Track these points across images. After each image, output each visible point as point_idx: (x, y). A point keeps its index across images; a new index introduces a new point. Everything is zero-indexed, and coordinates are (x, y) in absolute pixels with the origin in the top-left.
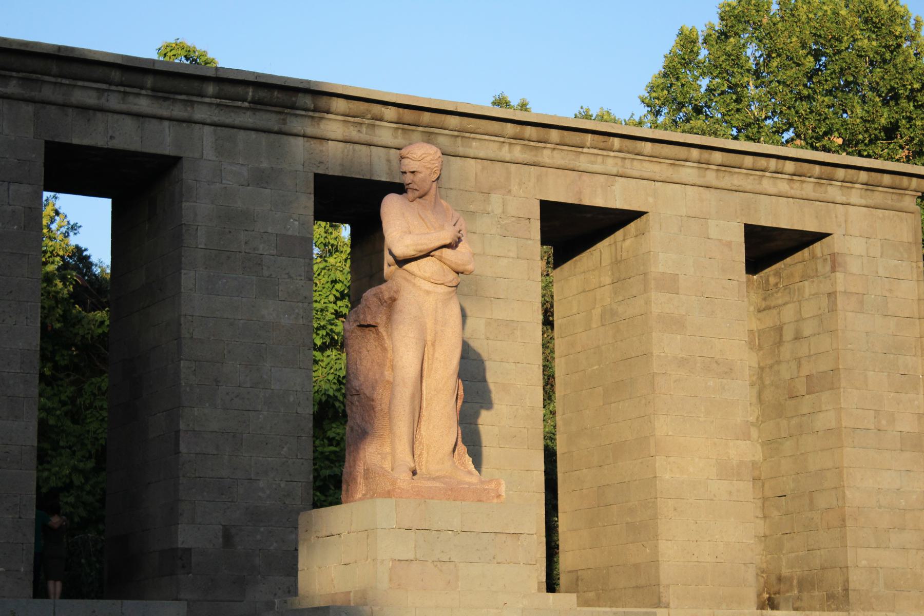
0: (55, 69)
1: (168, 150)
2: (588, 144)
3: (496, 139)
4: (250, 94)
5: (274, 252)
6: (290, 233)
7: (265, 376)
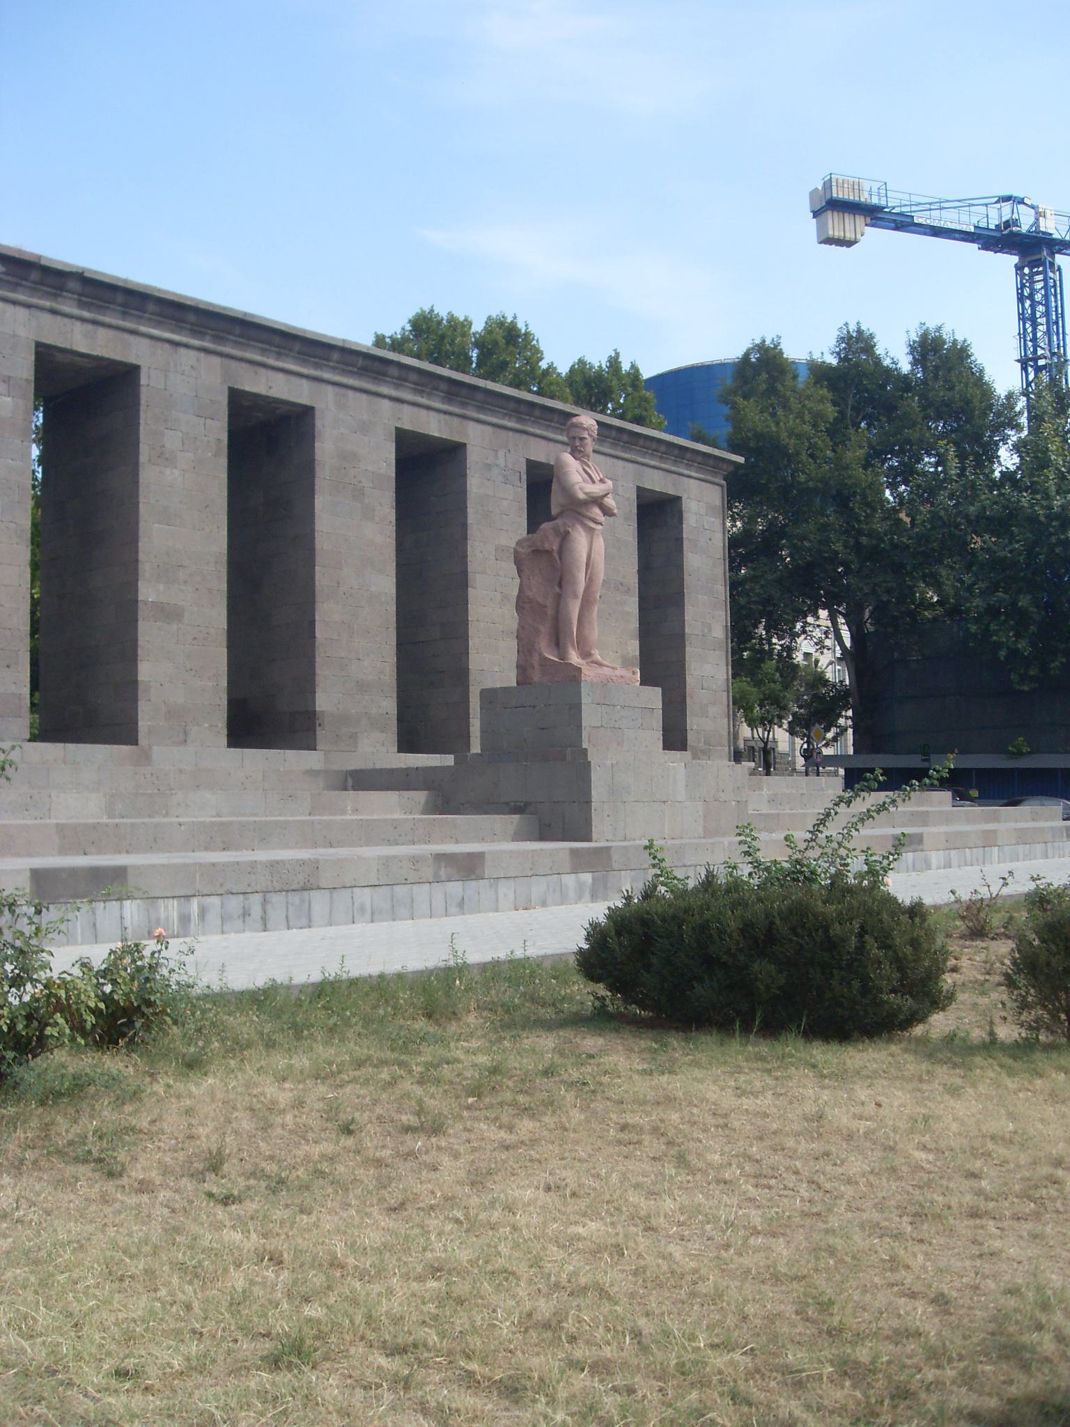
0: (238, 330)
1: (304, 400)
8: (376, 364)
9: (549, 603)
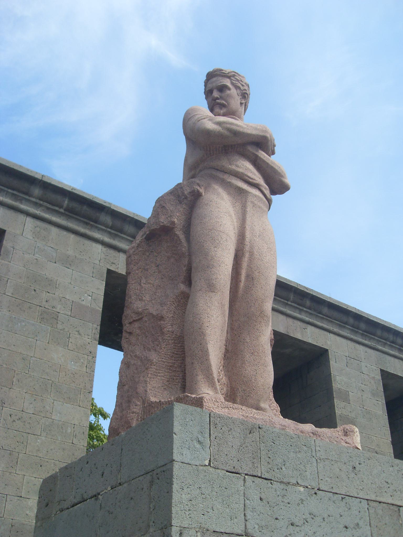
2: (291, 299)
4: (66, 202)
5: (69, 313)
6: (84, 303)
7: (48, 407)
8: (85, 207)
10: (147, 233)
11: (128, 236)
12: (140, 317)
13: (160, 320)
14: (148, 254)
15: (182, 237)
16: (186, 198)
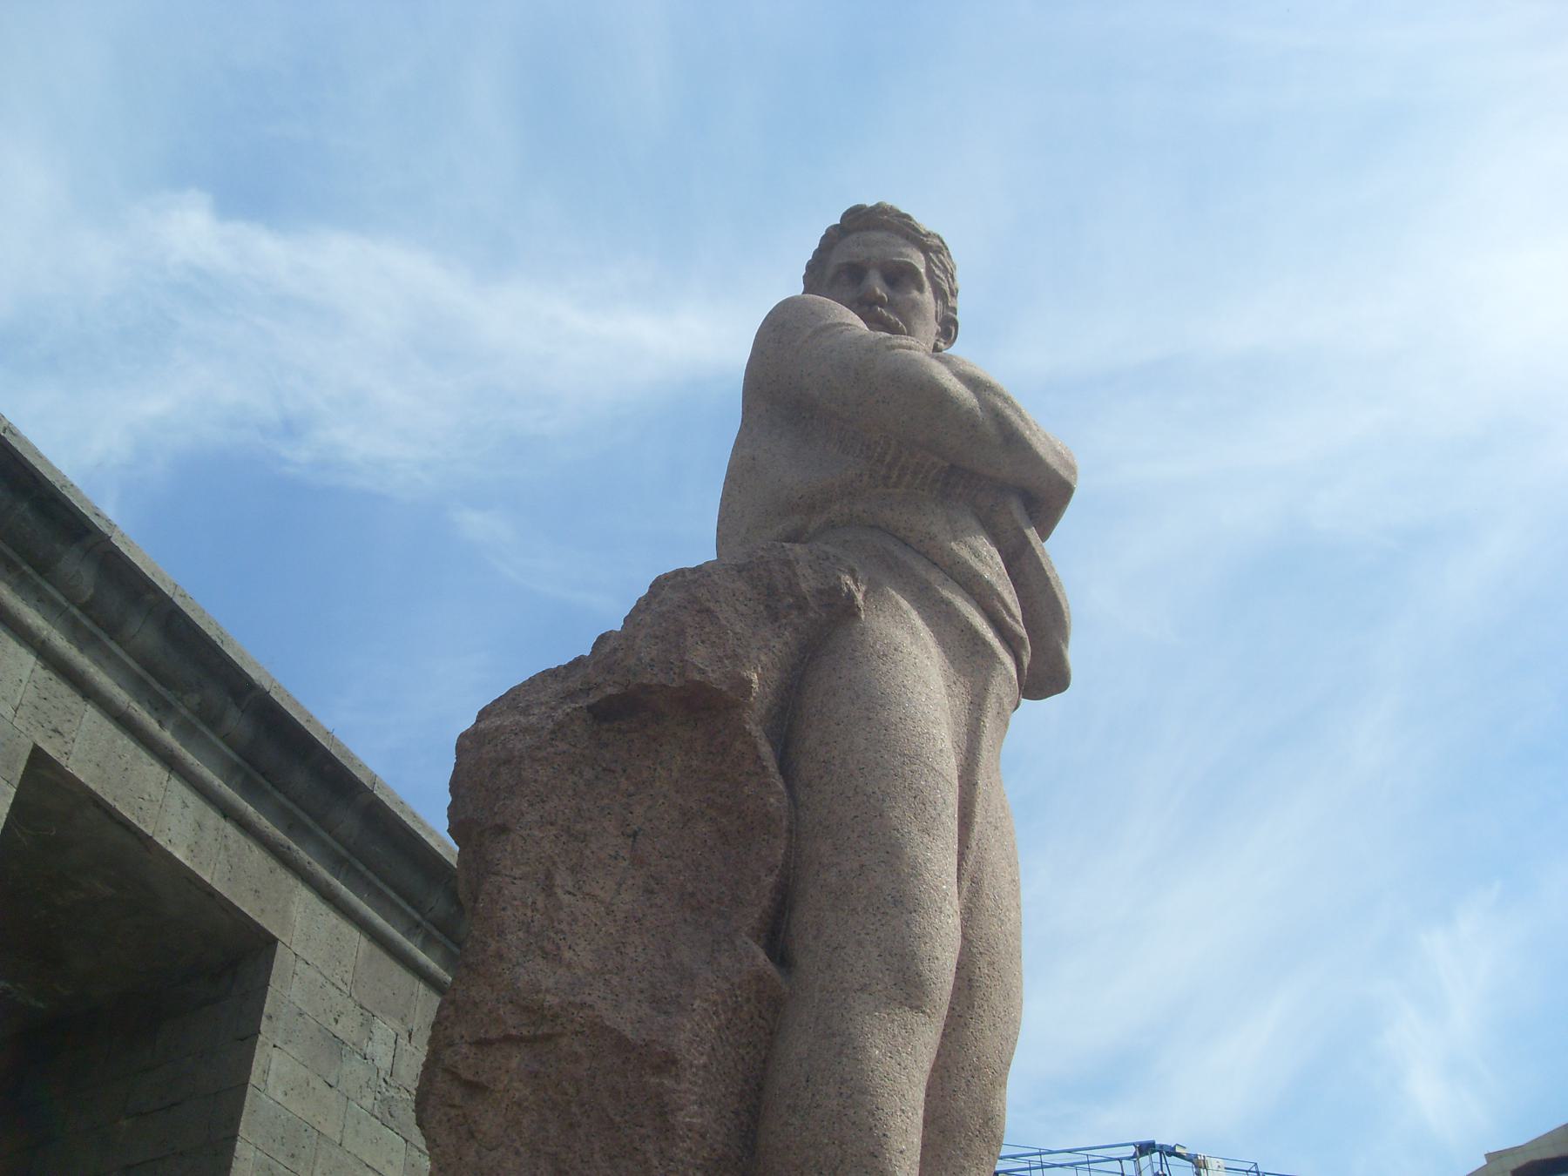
3: (409, 909)
8: (23, 507)
9: (694, 1035)
10: (610, 690)
11: (129, 653)
12: (545, 1029)
13: (658, 1070)
14: (589, 774)
15: (766, 749)
16: (801, 606)
